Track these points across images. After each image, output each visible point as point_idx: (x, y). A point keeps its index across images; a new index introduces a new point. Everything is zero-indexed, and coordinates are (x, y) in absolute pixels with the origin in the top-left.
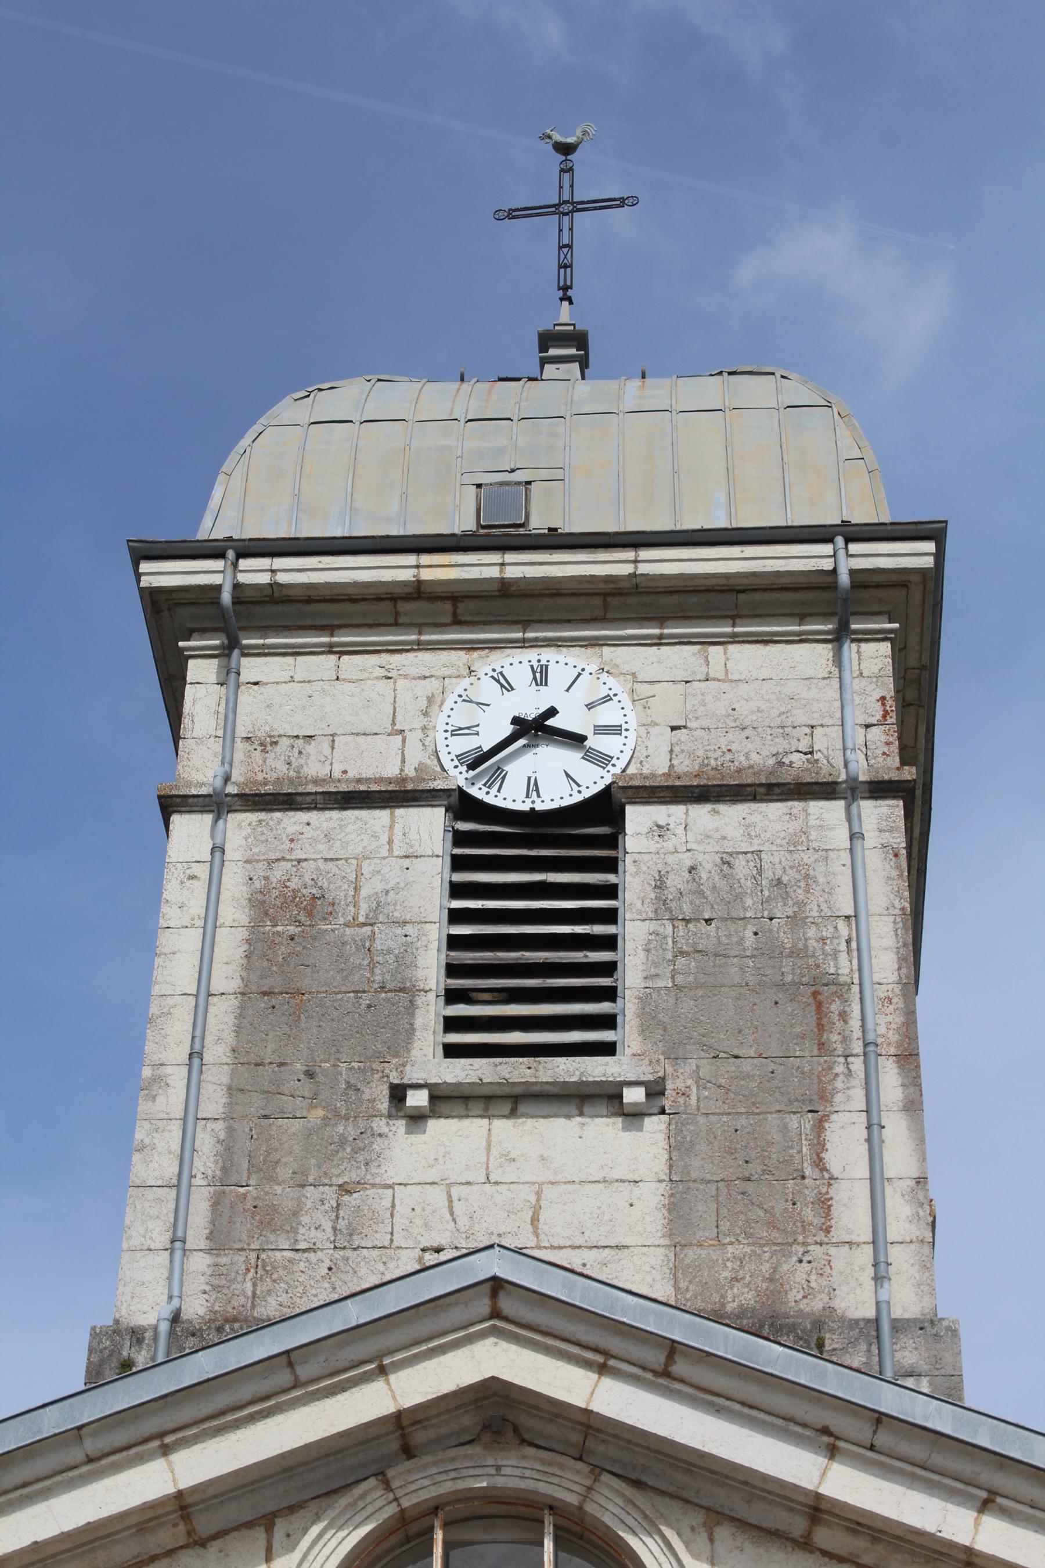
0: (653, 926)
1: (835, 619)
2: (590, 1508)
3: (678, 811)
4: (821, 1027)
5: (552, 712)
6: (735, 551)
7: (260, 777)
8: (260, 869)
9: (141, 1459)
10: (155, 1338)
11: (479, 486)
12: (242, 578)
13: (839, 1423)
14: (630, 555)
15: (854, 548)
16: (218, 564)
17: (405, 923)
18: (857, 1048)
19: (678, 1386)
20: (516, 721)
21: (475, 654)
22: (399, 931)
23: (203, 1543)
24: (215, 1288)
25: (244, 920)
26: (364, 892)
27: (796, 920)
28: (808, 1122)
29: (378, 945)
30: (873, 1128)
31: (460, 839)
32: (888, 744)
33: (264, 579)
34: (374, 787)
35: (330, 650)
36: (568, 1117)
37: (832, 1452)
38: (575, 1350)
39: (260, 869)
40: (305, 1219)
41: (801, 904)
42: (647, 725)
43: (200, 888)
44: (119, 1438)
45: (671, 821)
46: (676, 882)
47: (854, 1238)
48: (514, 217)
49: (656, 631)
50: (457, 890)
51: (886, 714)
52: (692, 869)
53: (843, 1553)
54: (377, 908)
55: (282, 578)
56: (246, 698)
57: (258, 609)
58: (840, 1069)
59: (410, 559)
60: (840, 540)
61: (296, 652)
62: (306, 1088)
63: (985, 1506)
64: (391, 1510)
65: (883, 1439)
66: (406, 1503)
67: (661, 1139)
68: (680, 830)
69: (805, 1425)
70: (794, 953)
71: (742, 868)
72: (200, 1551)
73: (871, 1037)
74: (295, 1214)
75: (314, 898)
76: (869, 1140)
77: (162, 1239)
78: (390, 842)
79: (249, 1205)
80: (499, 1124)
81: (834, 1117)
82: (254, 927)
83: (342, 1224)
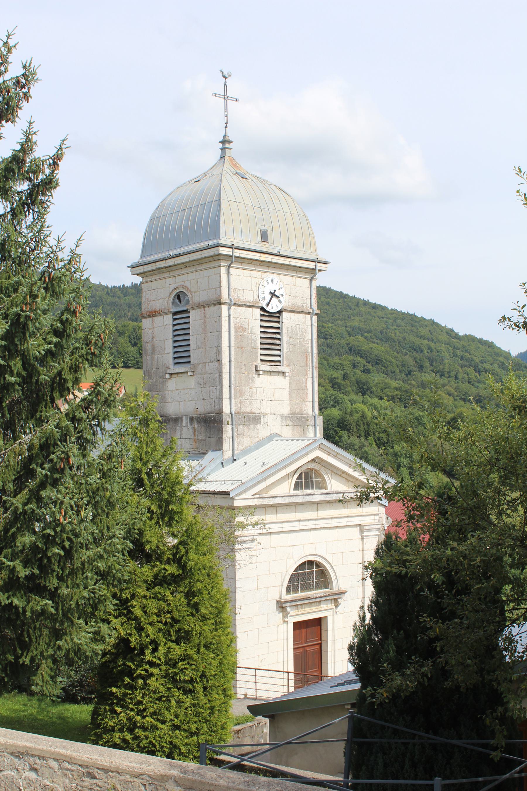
3: (290, 314)
27: (304, 339)
31: (262, 315)
35: (242, 269)
41: (305, 336)
46: (290, 329)
50: (262, 327)
54: (251, 331)
71: (298, 328)
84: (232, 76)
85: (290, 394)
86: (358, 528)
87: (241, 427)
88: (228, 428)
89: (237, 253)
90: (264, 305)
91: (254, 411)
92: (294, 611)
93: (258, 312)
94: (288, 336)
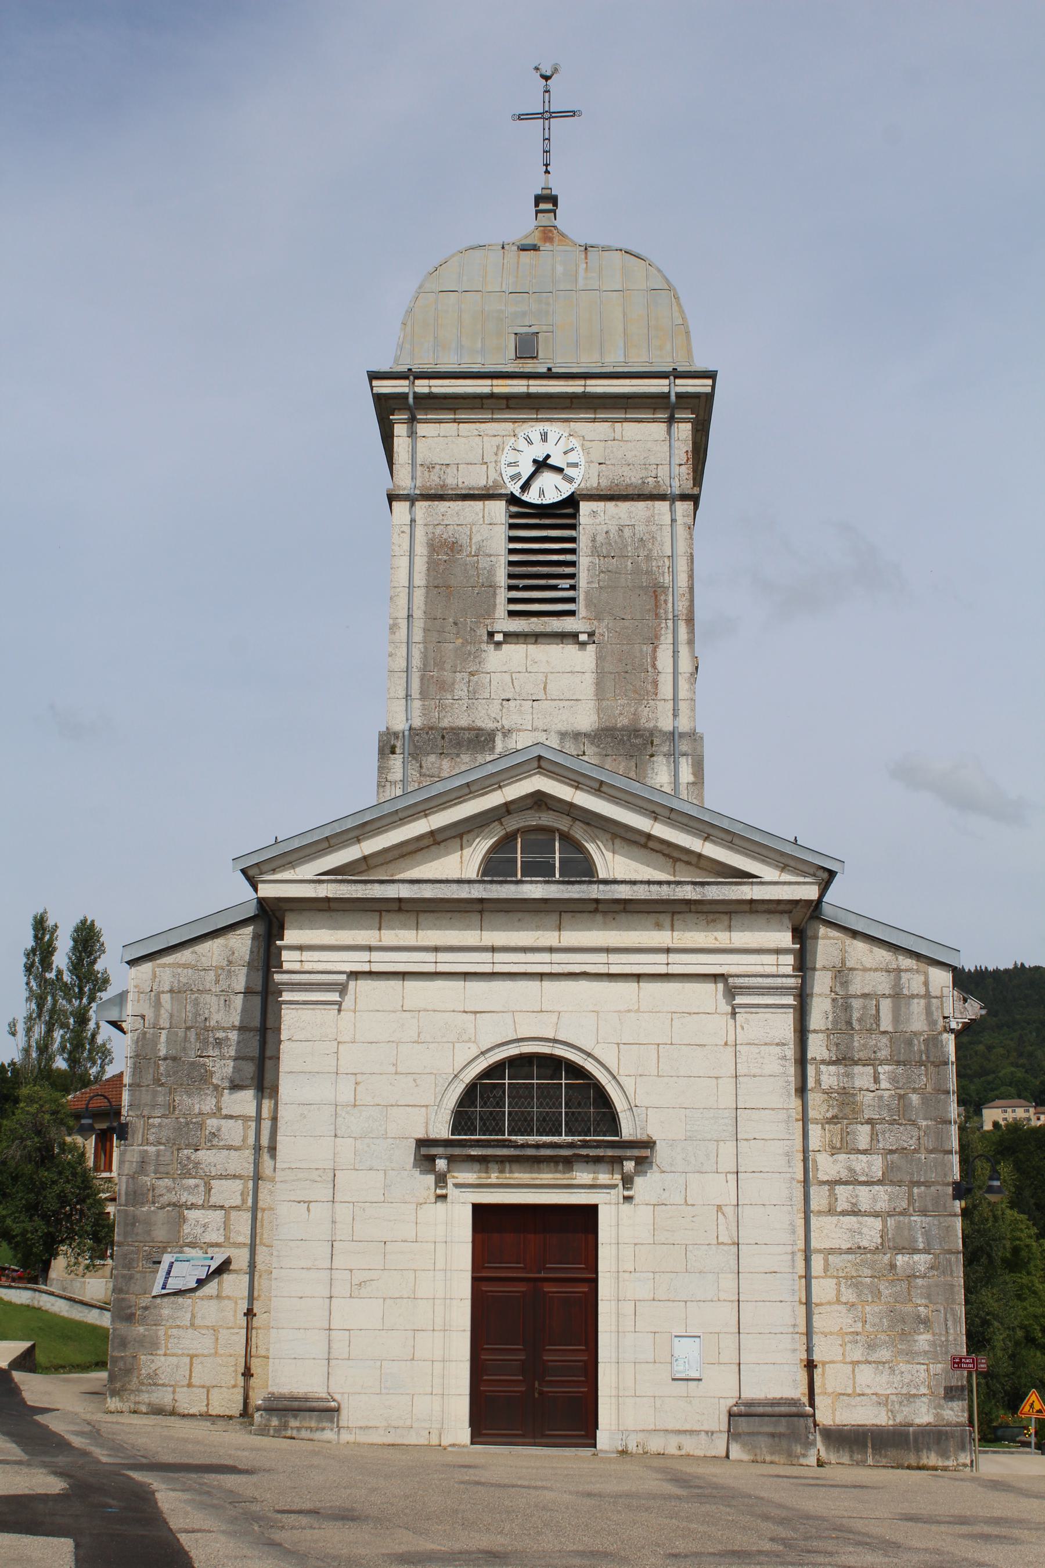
0: (589, 559)
1: (669, 411)
2: (571, 832)
3: (601, 504)
4: (656, 606)
5: (548, 457)
6: (627, 382)
7: (428, 484)
8: (430, 529)
9: (418, 819)
10: (404, 736)
11: (516, 334)
12: (417, 390)
13: (658, 810)
14: (582, 382)
15: (678, 381)
16: (406, 382)
17: (491, 555)
18: (671, 617)
19: (603, 795)
20: (535, 461)
21: (516, 424)
22: (488, 559)
23: (439, 843)
24: (424, 714)
25: (425, 553)
26: (474, 541)
27: (648, 558)
28: (650, 648)
29: (480, 566)
30: (675, 653)
31: (512, 516)
32: (688, 474)
33: (426, 390)
34: (476, 492)
35: (454, 421)
36: (557, 644)
37: (656, 819)
38: (568, 781)
39: (430, 529)
40: (457, 686)
41: (650, 550)
42: (589, 462)
43: (406, 537)
44: (410, 812)
45: (599, 509)
46: (600, 539)
47: (666, 698)
48: (522, 119)
49: (593, 416)
50: (512, 539)
51: (688, 459)
52: (607, 532)
53: (658, 849)
54: (479, 549)
55: (435, 390)
56: (421, 444)
57: (423, 401)
58: (663, 625)
59: (488, 382)
60: (672, 378)
61: (440, 422)
62: (454, 630)
63: (706, 839)
64: (503, 833)
65: (673, 816)
66: (508, 830)
67: (593, 654)
68: (602, 514)
69: (646, 810)
70: (647, 572)
71: (627, 532)
72: (437, 846)
73: (676, 613)
74: (453, 684)
75: (453, 543)
76: (673, 657)
77: (402, 693)
78: (483, 517)
79: (435, 680)
80: (530, 646)
81: (660, 646)
82: (430, 557)
83: (471, 689)
85: (597, 684)
86: (721, 986)
87: (432, 758)
88: (391, 762)
89: (423, 387)
90: (515, 489)
91: (479, 724)
92: (475, 1176)
93: (499, 508)
94: (595, 551)
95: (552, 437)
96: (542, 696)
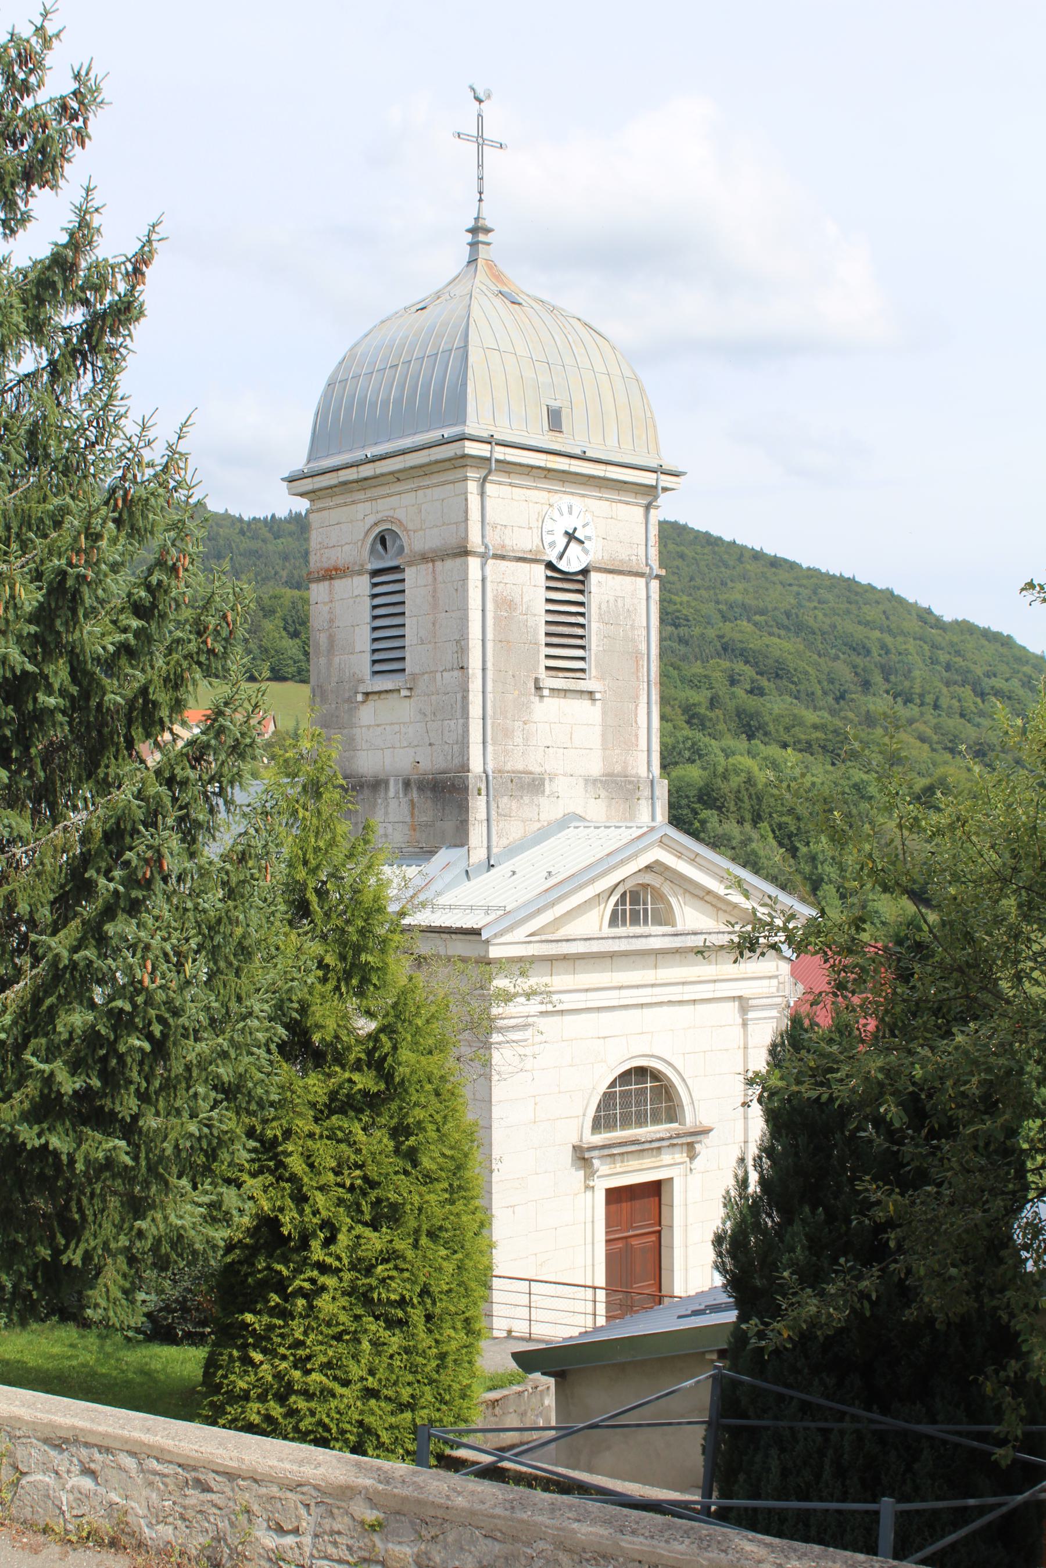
3: (604, 575)
27: (633, 627)
31: (548, 578)
35: (510, 484)
46: (604, 606)
50: (549, 601)
71: (620, 604)
84: (493, 97)
85: (603, 735)
87: (505, 799)
89: (500, 453)
91: (531, 768)
93: (540, 572)
94: (601, 619)
95: (575, 511)
96: (568, 745)
